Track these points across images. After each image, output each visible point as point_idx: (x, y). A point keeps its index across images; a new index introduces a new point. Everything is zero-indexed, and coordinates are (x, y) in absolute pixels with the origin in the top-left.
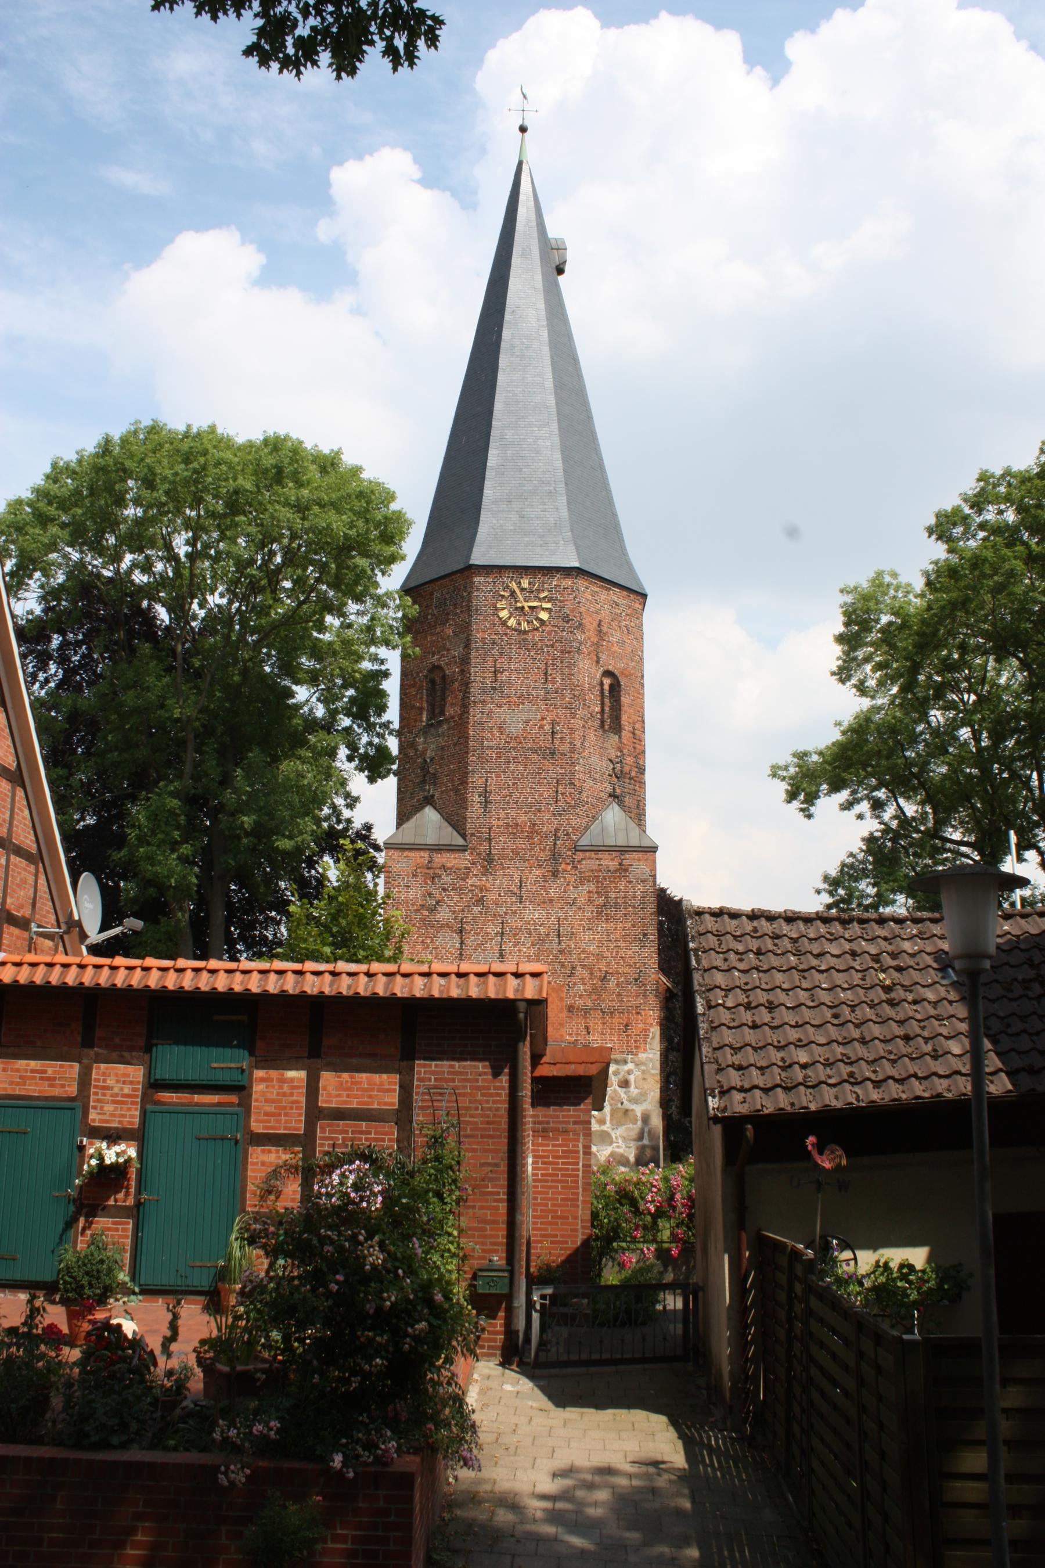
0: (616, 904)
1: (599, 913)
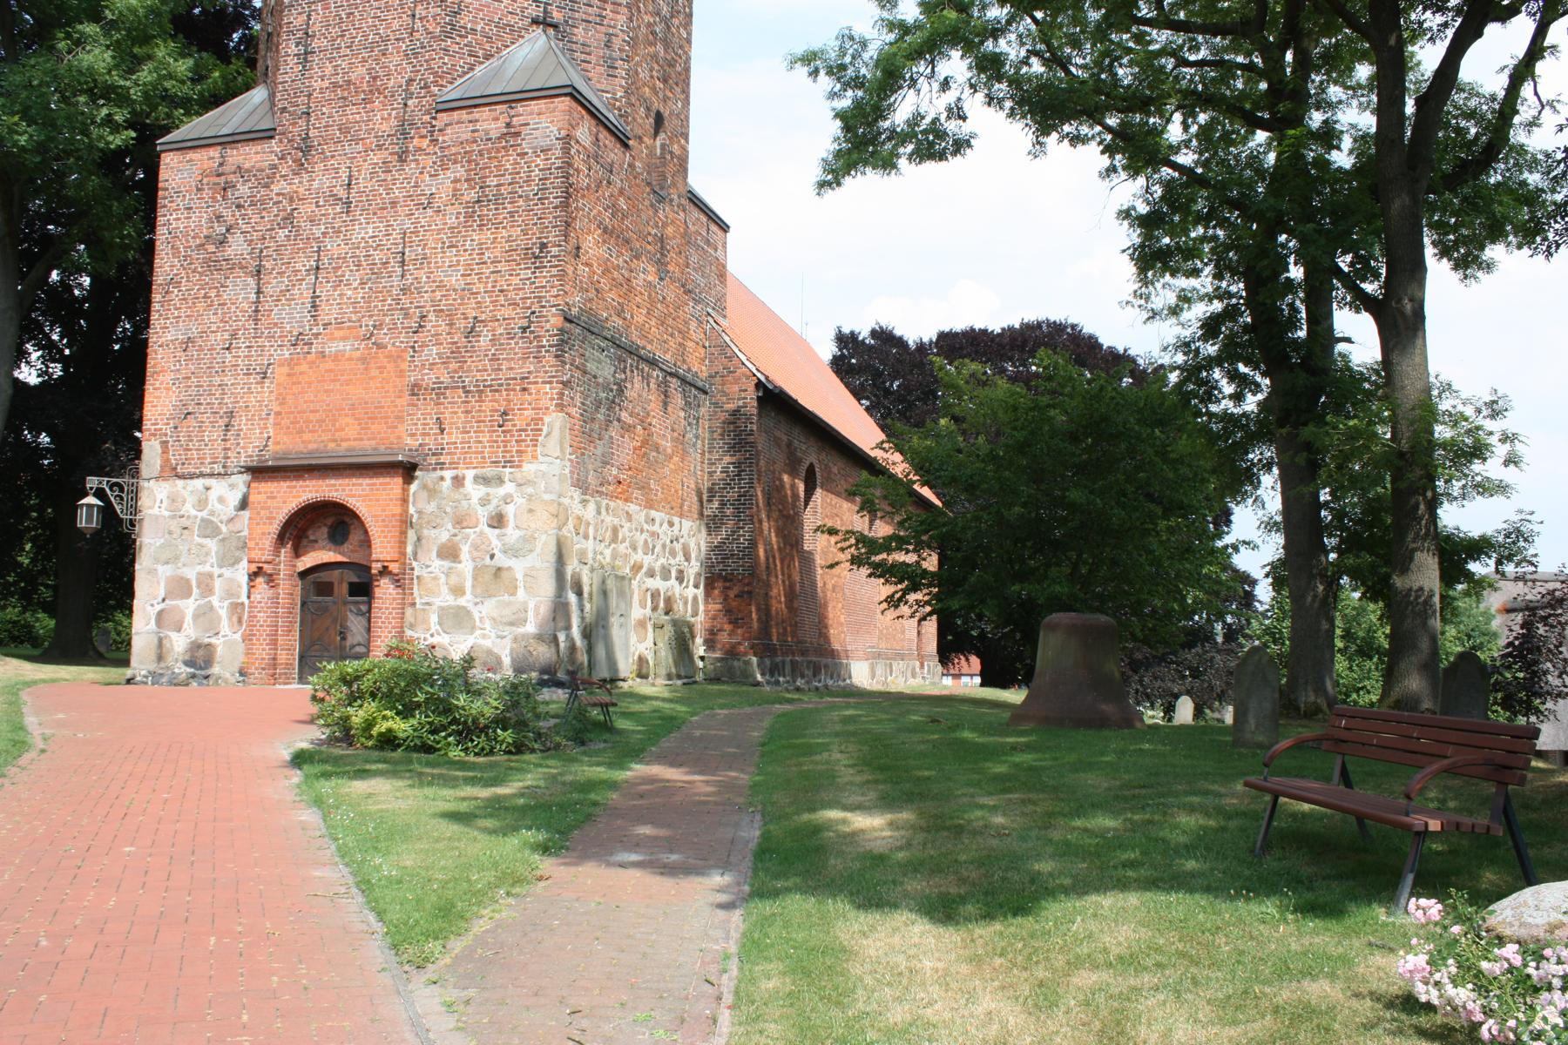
0: (498, 196)
1: (469, 216)
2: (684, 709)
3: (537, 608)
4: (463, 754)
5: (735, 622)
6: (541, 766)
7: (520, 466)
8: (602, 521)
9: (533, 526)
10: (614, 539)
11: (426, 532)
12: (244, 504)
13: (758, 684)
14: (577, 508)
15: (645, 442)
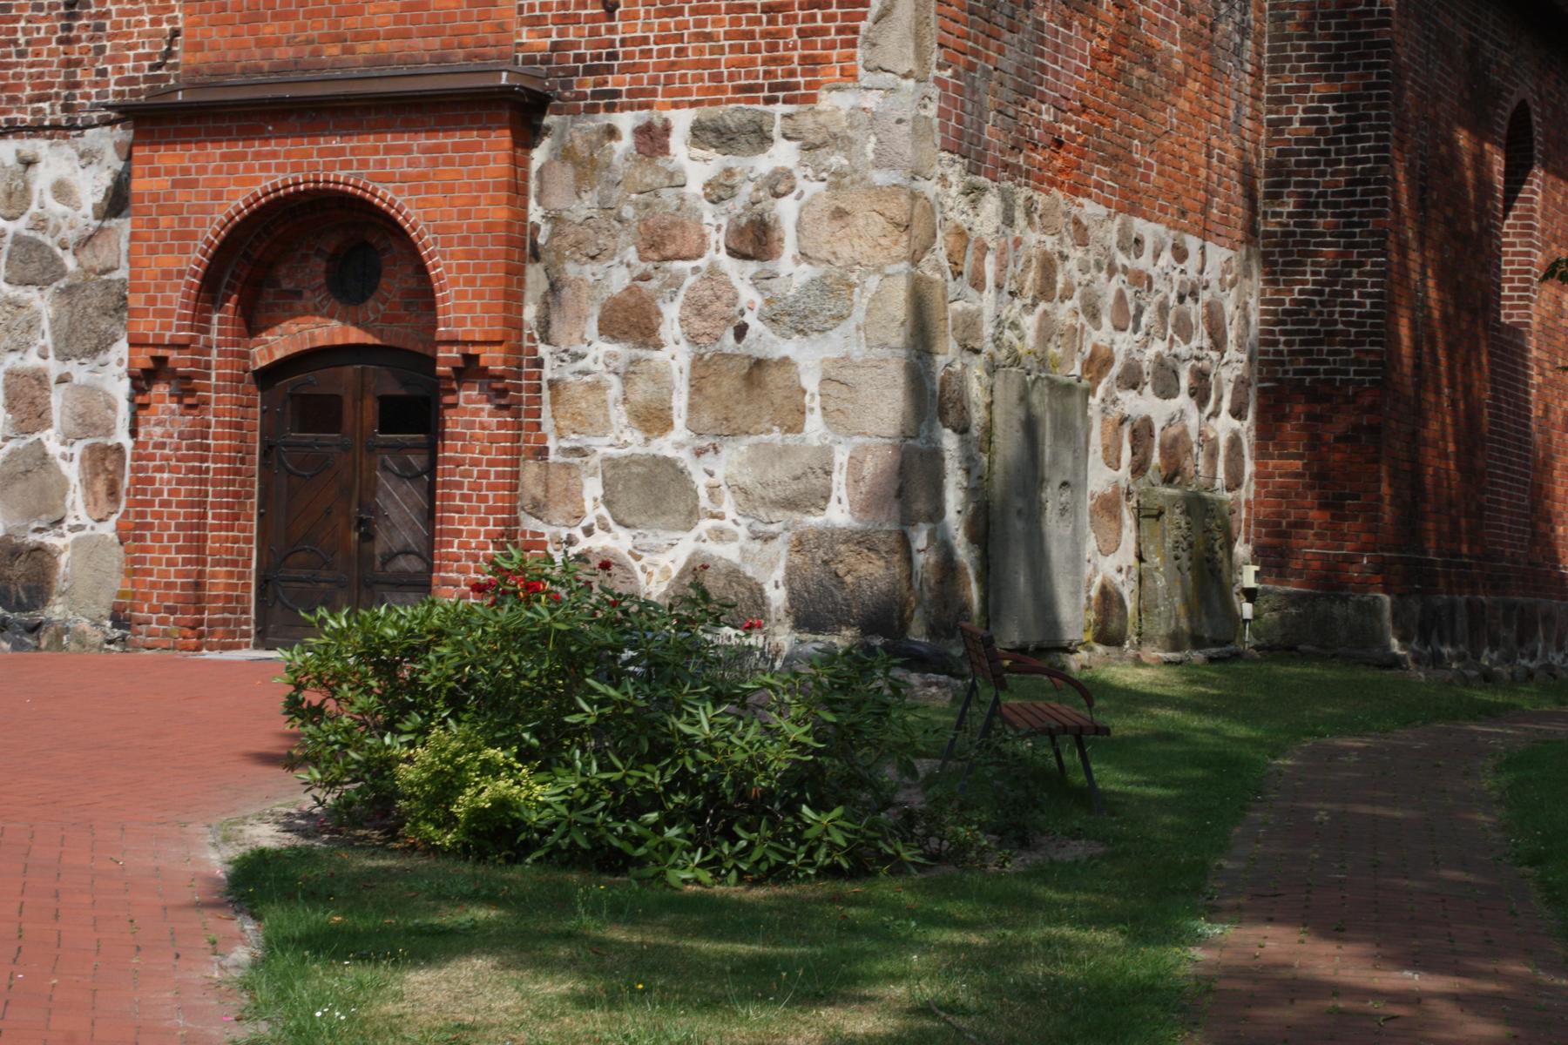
2: (1241, 731)
3: (855, 463)
4: (705, 876)
5: (1332, 504)
6: (932, 920)
7: (811, 99)
8: (1018, 242)
9: (845, 251)
10: (1046, 290)
11: (571, 270)
12: (117, 201)
13: (1395, 662)
14: (955, 207)
15: (1120, 41)
